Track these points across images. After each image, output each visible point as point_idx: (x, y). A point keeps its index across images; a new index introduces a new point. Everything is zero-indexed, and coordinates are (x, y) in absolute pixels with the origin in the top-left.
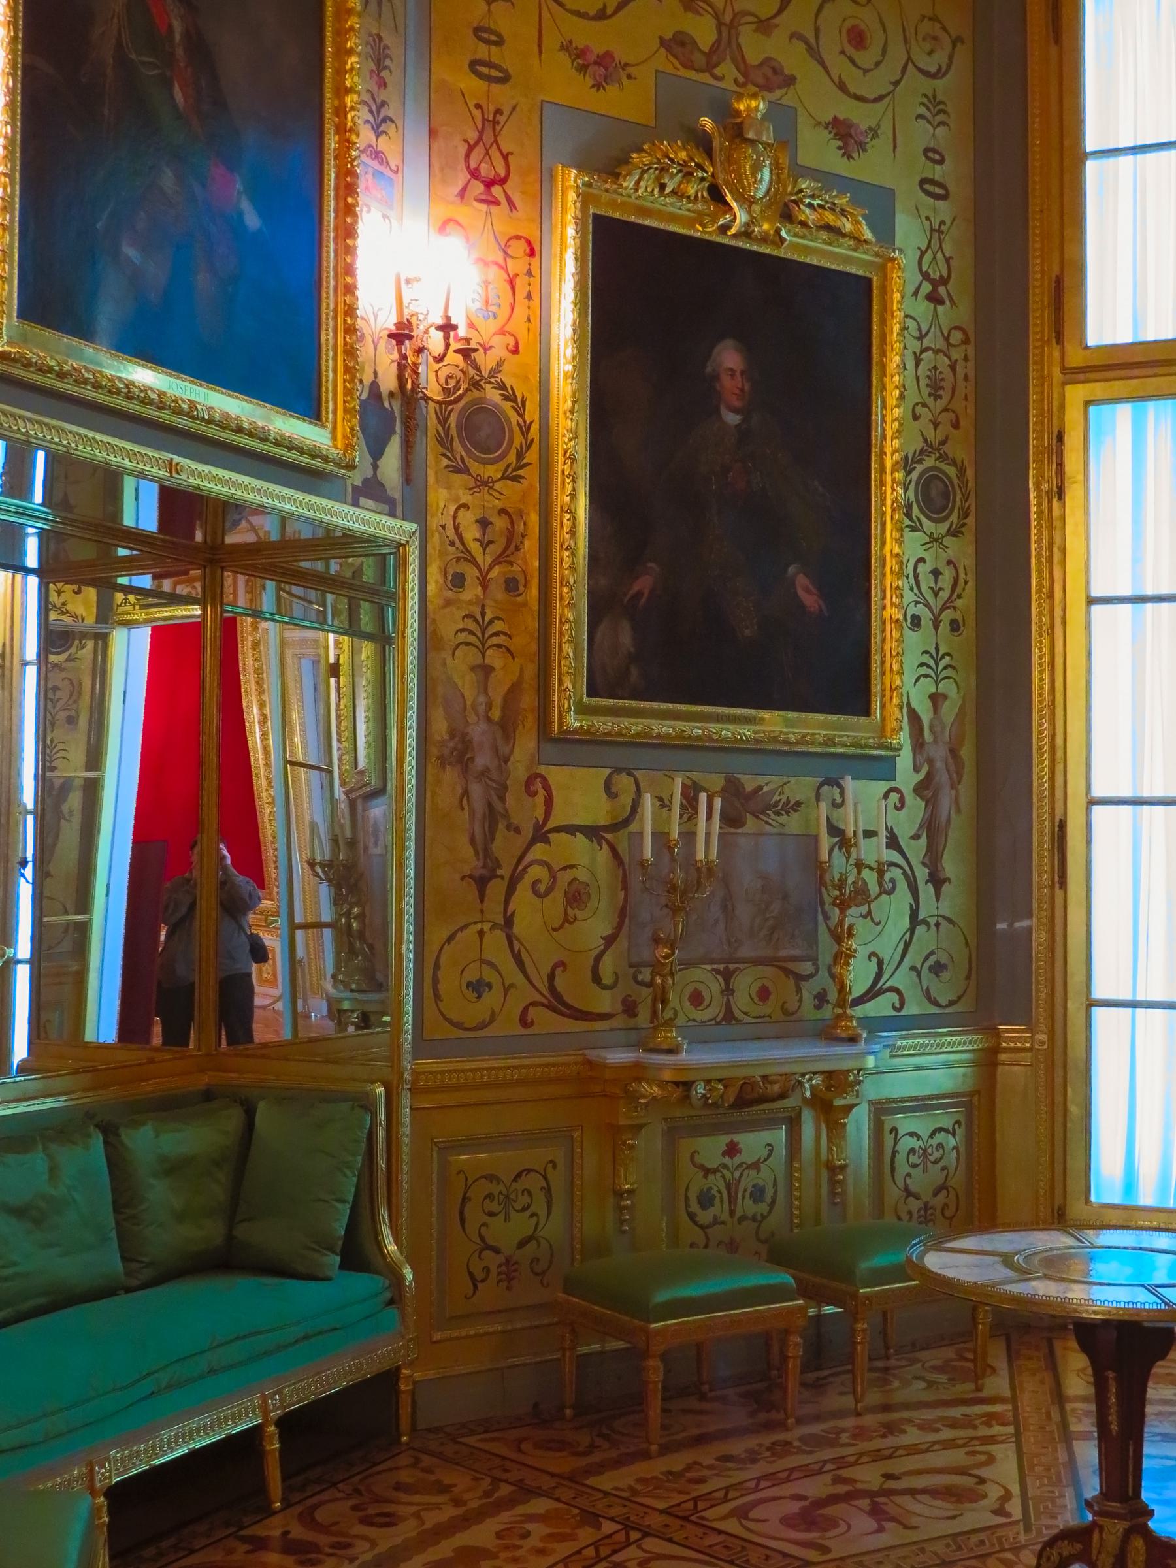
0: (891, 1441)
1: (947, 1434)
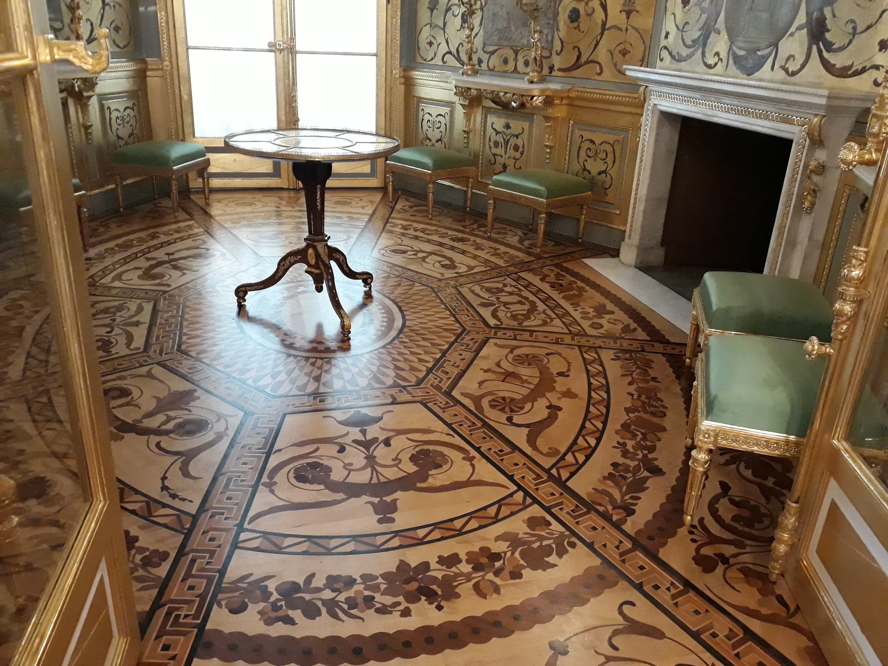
0: (155, 242)
1: (176, 236)
